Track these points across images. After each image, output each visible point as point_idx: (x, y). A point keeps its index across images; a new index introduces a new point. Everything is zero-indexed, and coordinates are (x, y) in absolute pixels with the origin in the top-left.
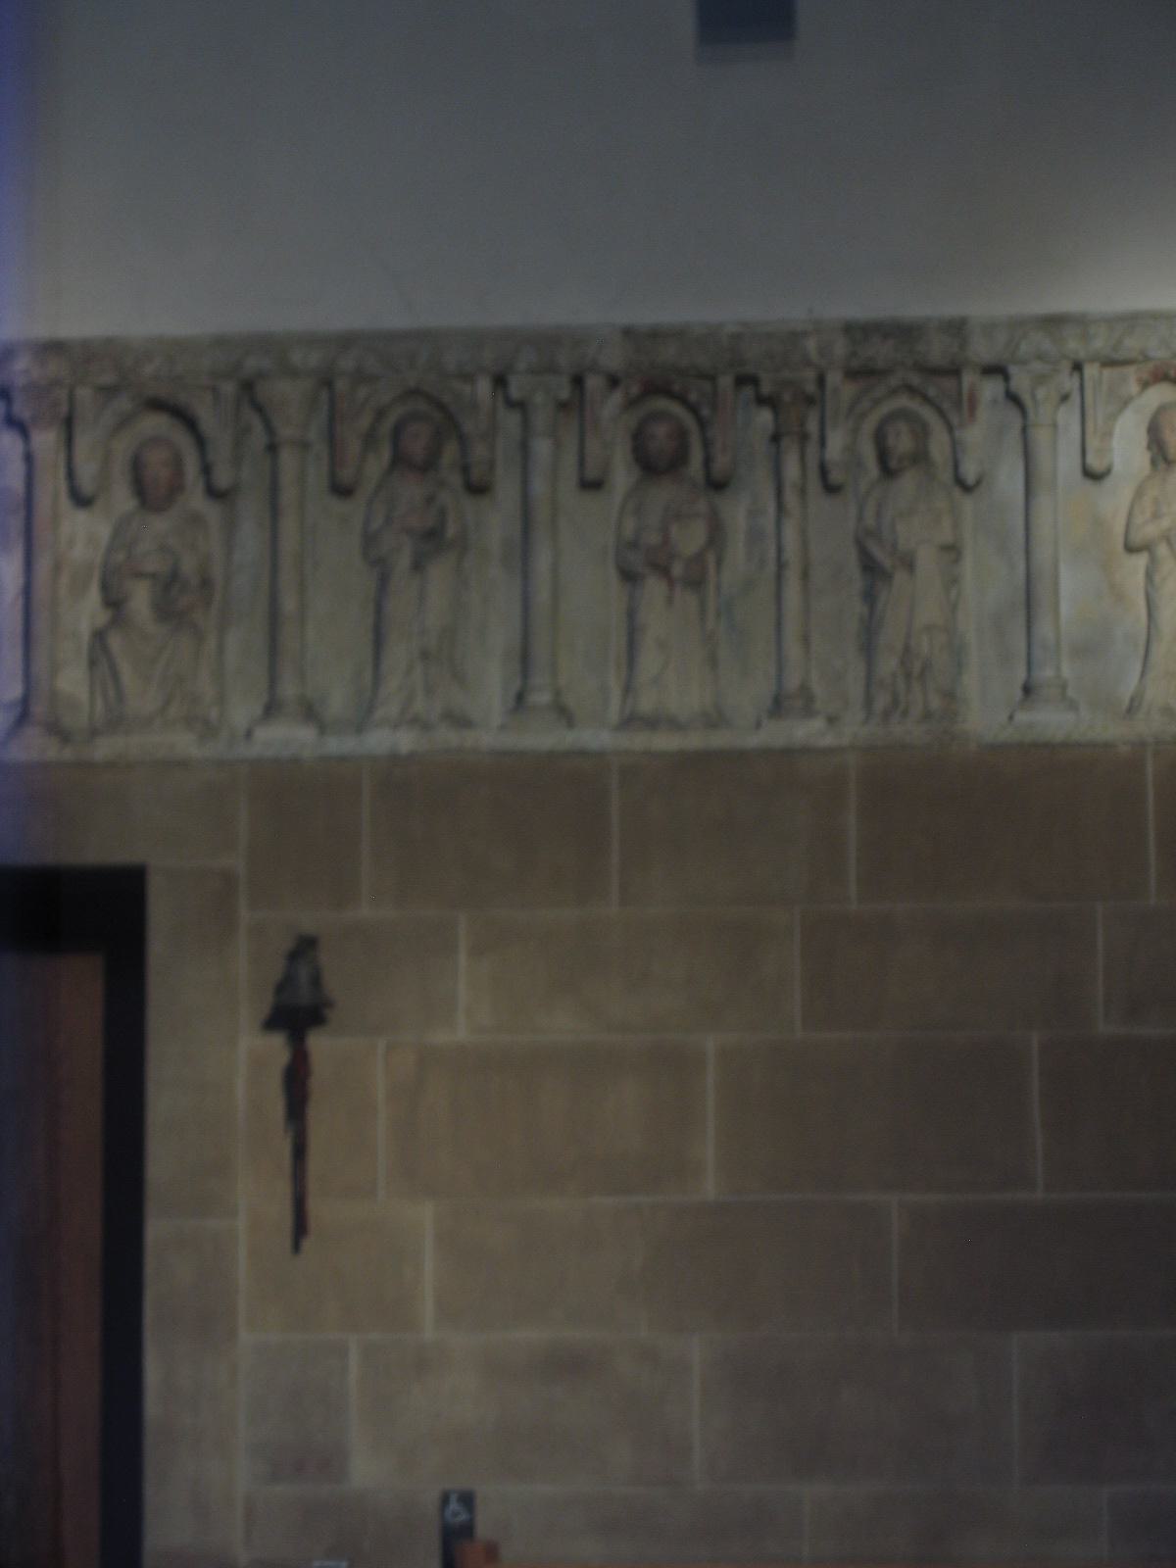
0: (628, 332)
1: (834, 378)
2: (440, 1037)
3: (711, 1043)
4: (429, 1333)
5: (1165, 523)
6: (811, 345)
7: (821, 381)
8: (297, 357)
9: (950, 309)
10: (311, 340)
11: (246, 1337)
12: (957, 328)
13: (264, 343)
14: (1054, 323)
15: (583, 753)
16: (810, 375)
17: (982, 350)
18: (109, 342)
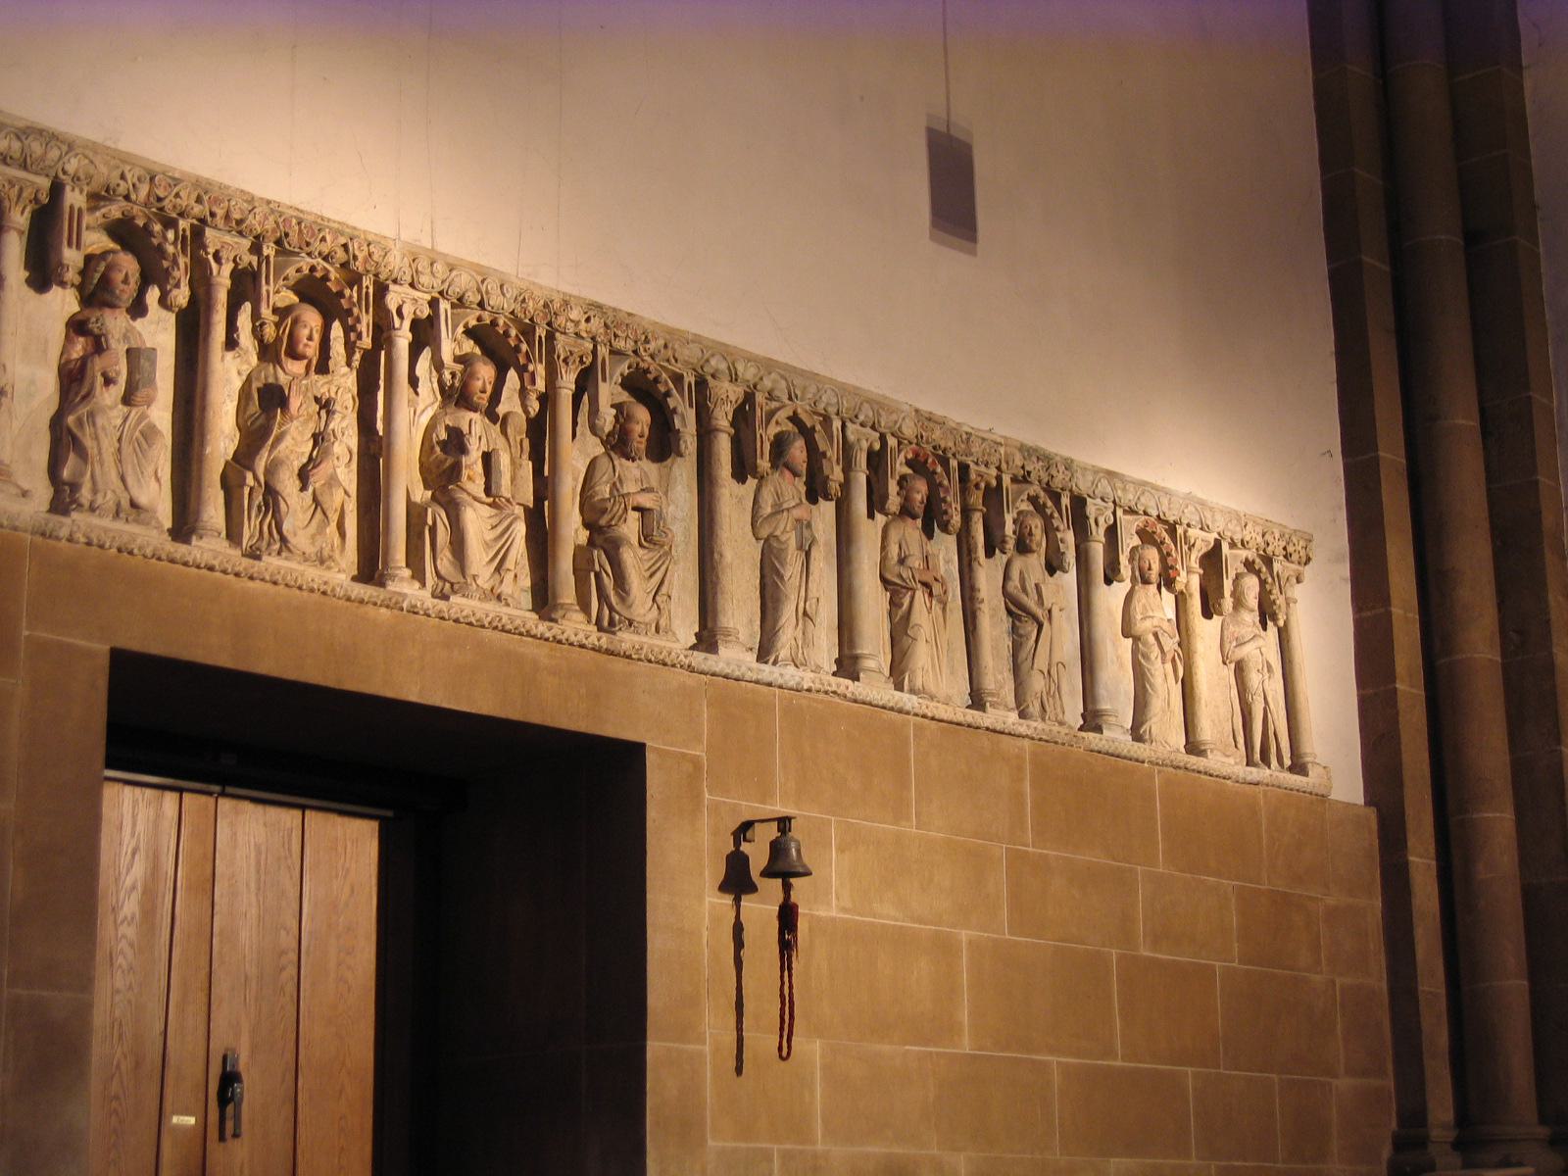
0: (917, 411)
1: (1006, 479)
2: (822, 913)
3: (964, 935)
4: (820, 1147)
5: (1155, 622)
6: (1002, 450)
7: (999, 479)
8: (740, 368)
9: (1065, 452)
10: (750, 359)
11: (710, 1143)
12: (1069, 465)
13: (726, 352)
14: (1111, 475)
15: (900, 711)
16: (993, 472)
17: (1083, 485)
18: (630, 314)
